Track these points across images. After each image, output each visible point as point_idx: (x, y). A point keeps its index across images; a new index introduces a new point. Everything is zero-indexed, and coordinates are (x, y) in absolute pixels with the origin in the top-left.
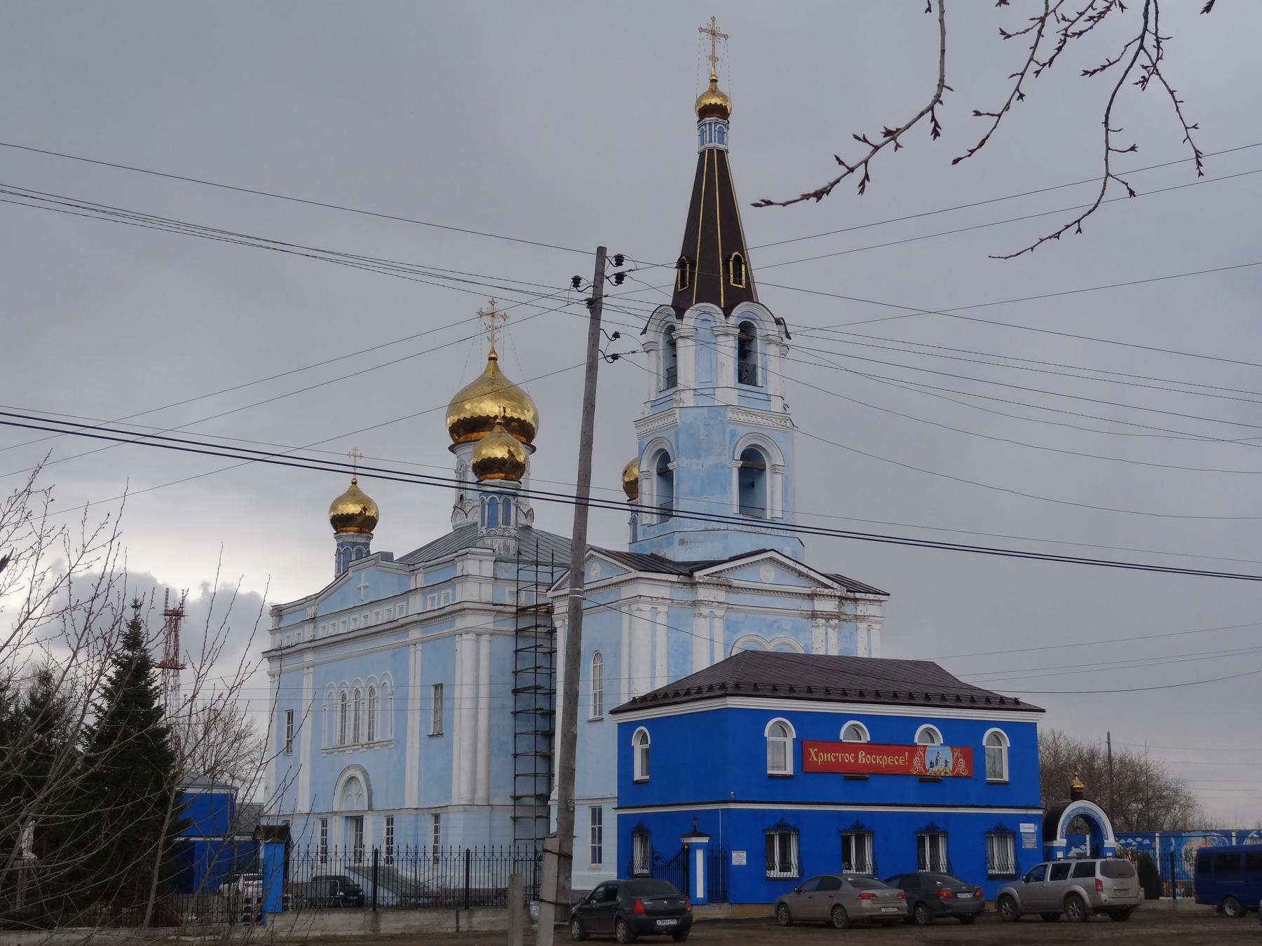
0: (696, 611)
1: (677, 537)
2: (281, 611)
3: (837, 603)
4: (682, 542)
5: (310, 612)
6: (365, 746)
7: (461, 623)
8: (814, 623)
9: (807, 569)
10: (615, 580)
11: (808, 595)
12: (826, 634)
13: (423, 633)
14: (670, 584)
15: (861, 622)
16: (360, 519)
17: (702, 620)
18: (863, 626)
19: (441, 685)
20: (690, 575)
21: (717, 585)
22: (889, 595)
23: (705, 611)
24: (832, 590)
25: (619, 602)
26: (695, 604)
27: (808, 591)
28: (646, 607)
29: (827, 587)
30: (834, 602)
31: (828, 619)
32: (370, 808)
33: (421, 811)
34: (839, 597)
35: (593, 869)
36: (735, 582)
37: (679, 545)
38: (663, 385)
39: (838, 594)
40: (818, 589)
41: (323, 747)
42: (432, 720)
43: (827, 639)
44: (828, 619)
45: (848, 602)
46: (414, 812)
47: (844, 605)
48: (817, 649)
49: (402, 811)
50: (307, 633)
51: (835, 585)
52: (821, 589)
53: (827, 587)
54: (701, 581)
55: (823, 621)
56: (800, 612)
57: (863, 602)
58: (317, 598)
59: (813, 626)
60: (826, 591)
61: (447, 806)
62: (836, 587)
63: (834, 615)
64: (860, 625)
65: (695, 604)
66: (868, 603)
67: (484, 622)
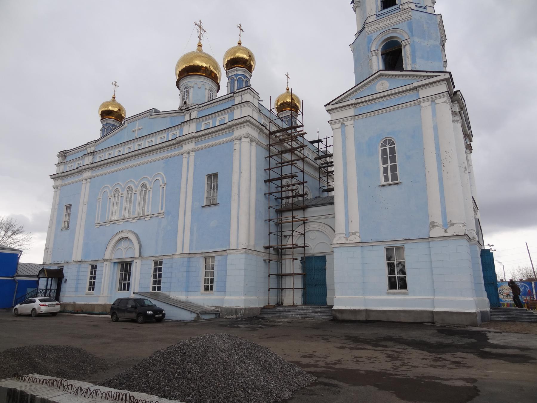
2: (66, 153)
5: (90, 150)
6: (135, 218)
7: (238, 133)
10: (415, 84)
13: (196, 145)
16: (116, 114)
19: (216, 175)
25: (418, 100)
32: (140, 255)
33: (191, 256)
35: (388, 294)
38: (380, 9)
41: (96, 222)
42: (205, 196)
46: (187, 256)
49: (174, 256)
50: (88, 160)
58: (96, 142)
61: (226, 250)
67: (255, 134)
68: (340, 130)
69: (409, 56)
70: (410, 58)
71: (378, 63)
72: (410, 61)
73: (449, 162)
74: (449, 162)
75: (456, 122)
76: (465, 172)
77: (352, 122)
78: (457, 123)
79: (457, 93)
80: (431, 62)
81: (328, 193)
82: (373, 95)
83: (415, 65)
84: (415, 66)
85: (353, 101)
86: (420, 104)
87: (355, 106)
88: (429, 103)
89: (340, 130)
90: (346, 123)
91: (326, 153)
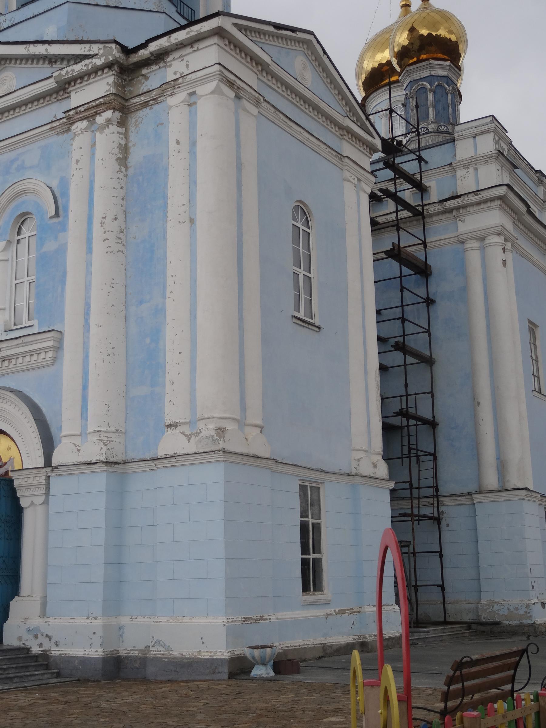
3: (111, 80)
9: (46, 46)
12: (93, 145)
15: (172, 95)
24: (87, 61)
27: (51, 84)
29: (78, 59)
30: (105, 81)
31: (91, 118)
34: (109, 66)
39: (98, 62)
40: (64, 72)
43: (93, 155)
44: (91, 118)
45: (154, 67)
47: (146, 77)
51: (95, 49)
52: (69, 69)
53: (78, 59)
55: (84, 124)
56: (48, 127)
57: (176, 55)
60: (78, 68)
63: (100, 104)
64: (171, 101)
66: (188, 50)
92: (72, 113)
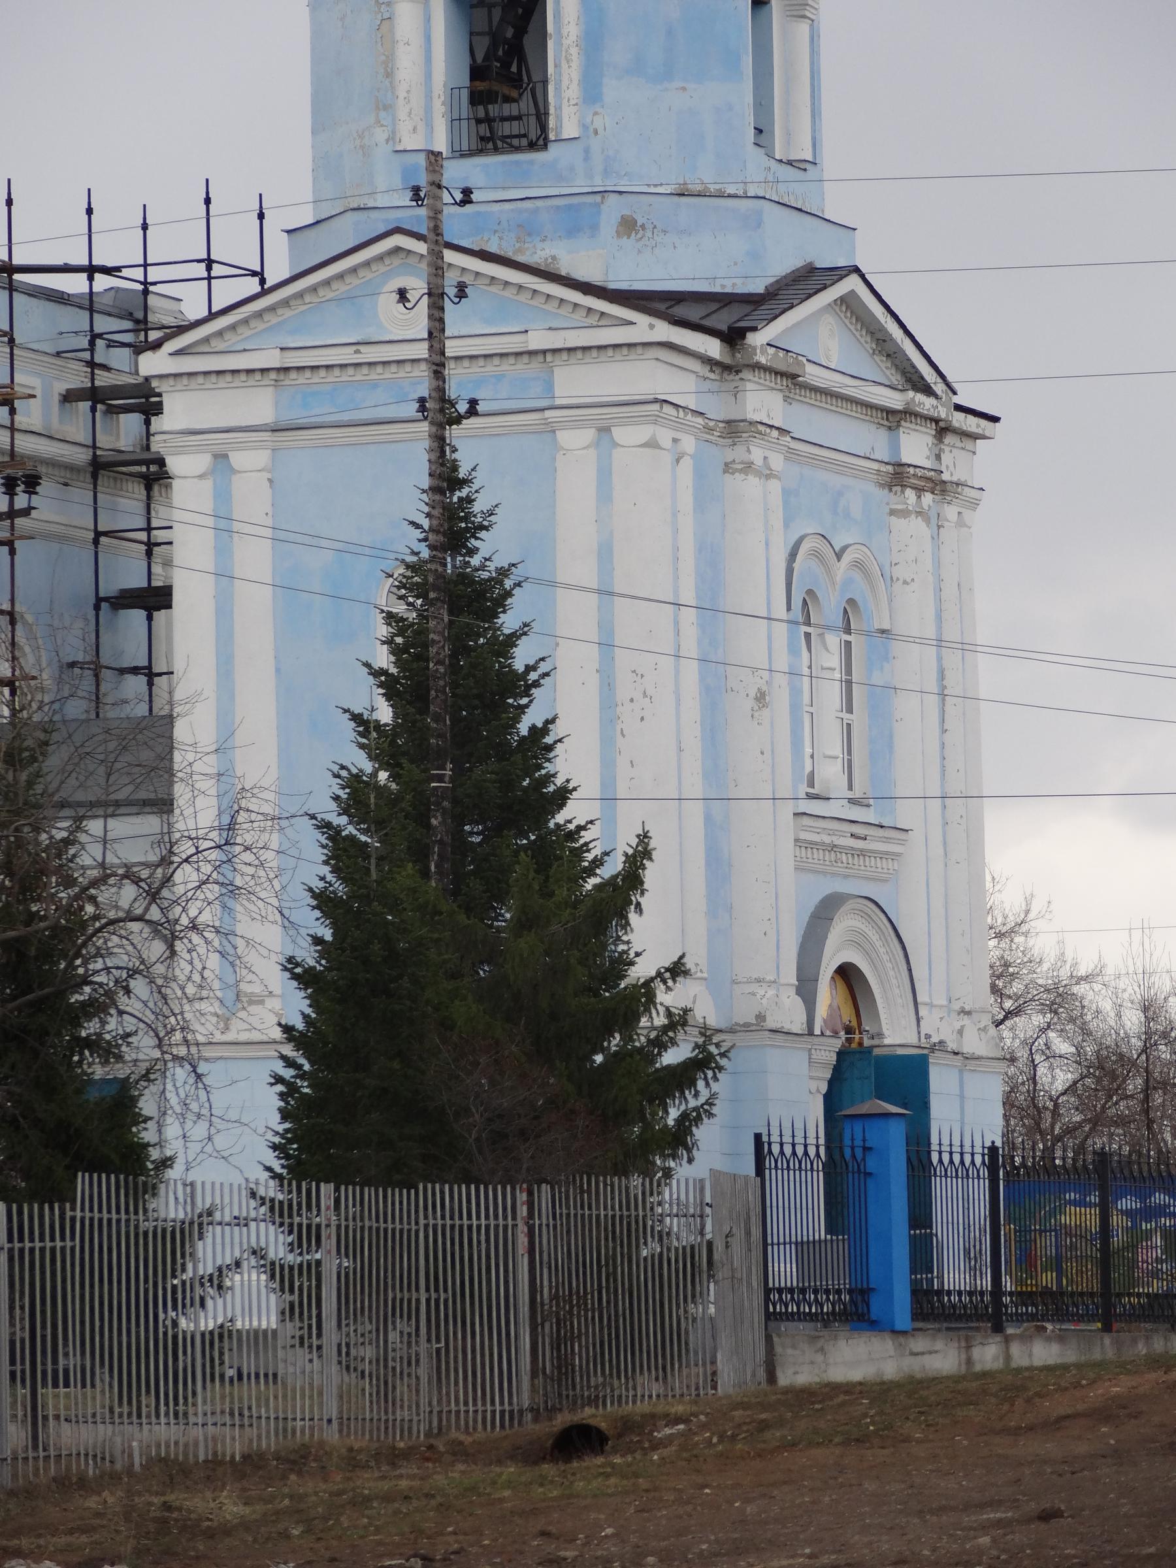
0: (738, 453)
1: (613, 210)
4: (628, 226)
8: (893, 500)
10: (537, 340)
11: (889, 412)
14: (695, 365)
17: (753, 480)
18: (951, 512)
20: (733, 337)
21: (776, 373)
22: (995, 419)
23: (757, 455)
25: (548, 414)
26: (733, 429)
28: (665, 436)
29: (928, 391)
36: (810, 368)
37: (619, 234)
44: (920, 491)
48: (905, 582)
53: (928, 391)
54: (763, 360)
56: (875, 466)
59: (892, 512)
60: (925, 404)
62: (939, 392)
65: (733, 429)
68: (208, 484)
69: (574, 51)
70: (575, 64)
71: (428, 39)
72: (576, 82)
73: (642, 719)
74: (642, 719)
75: (741, 471)
76: (756, 714)
77: (261, 458)
78: (743, 476)
79: (744, 337)
80: (684, 89)
81: (150, 618)
82: (362, 348)
83: (596, 113)
84: (596, 117)
85: (272, 359)
86: (554, 431)
87: (282, 377)
88: (589, 435)
89: (208, 484)
90: (238, 459)
91: (139, 315)
92: (911, 470)
